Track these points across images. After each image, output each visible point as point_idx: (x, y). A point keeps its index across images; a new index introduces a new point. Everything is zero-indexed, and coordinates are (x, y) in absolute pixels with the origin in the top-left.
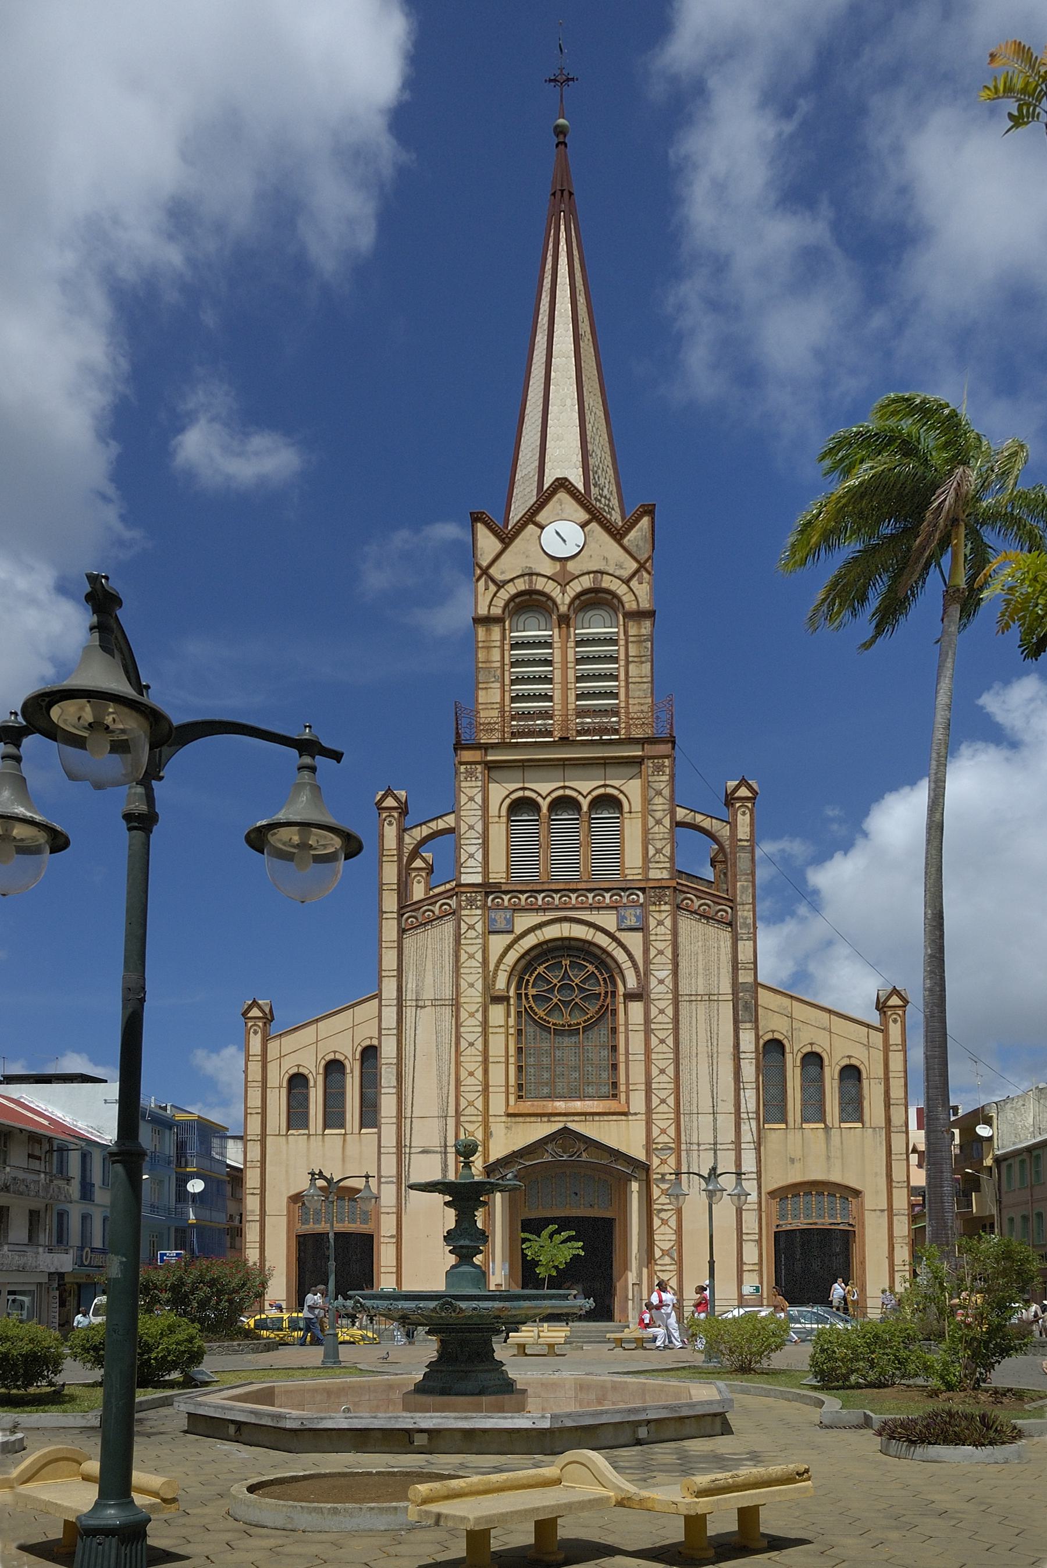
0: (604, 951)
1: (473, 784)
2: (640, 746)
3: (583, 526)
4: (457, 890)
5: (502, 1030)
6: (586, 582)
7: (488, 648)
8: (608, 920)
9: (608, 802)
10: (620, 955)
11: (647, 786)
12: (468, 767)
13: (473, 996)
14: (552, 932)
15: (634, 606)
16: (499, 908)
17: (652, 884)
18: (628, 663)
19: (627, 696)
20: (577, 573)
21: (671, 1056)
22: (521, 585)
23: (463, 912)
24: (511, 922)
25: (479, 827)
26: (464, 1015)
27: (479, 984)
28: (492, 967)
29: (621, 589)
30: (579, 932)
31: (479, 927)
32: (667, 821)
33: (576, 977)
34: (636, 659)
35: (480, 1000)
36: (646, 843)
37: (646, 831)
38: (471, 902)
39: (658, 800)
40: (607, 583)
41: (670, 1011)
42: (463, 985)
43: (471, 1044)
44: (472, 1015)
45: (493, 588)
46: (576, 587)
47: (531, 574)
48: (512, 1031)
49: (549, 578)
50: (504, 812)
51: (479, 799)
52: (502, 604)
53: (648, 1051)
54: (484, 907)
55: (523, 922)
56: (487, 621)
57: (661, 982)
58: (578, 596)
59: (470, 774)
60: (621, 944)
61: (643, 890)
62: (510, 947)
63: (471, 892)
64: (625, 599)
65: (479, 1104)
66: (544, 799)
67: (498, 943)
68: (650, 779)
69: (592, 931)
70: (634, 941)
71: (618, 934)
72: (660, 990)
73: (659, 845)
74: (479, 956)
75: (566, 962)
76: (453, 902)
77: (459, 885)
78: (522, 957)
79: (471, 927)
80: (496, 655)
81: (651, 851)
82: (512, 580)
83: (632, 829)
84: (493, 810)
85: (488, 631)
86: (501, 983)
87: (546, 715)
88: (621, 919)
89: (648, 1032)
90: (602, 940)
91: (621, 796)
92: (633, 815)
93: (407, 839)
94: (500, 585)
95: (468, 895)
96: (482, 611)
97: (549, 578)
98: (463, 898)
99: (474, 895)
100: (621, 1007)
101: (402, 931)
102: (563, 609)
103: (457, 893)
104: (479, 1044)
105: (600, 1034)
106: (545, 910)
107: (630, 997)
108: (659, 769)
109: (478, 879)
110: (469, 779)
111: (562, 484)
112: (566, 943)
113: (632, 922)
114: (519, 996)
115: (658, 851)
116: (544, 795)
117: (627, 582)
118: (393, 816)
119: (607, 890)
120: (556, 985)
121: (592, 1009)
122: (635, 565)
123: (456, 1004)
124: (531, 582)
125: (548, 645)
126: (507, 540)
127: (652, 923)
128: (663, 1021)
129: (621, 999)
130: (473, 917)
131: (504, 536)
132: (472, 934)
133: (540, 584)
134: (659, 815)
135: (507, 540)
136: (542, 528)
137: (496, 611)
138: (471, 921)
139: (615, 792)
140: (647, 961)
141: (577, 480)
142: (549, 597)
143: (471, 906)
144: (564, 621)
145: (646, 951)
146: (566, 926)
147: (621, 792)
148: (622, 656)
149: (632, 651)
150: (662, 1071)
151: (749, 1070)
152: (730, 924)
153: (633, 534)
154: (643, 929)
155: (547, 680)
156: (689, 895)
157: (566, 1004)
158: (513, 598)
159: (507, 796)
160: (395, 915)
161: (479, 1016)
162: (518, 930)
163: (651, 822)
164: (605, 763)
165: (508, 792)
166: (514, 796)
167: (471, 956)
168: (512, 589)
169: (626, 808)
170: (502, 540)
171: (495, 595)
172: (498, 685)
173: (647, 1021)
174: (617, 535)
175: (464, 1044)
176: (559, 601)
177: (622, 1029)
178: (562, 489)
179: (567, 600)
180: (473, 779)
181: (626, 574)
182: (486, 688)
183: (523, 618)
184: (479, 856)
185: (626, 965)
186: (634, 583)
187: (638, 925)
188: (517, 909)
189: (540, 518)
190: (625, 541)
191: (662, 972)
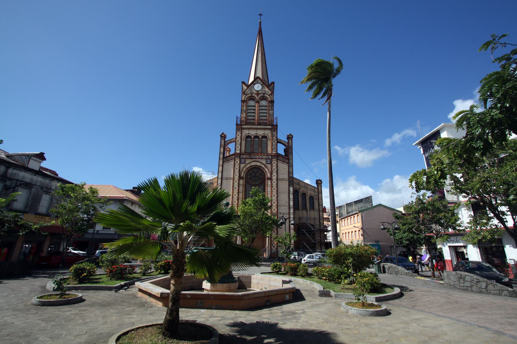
0: (263, 168)
3: (261, 85)
5: (242, 185)
6: (262, 95)
7: (244, 106)
9: (264, 137)
10: (266, 170)
11: (272, 134)
13: (237, 177)
14: (253, 164)
15: (270, 100)
16: (243, 158)
17: (273, 154)
18: (269, 110)
19: (269, 116)
21: (276, 192)
23: (236, 159)
24: (245, 161)
25: (240, 141)
26: (235, 181)
27: (238, 175)
28: (241, 171)
30: (258, 164)
31: (239, 162)
32: (276, 141)
33: (257, 174)
35: (238, 178)
36: (272, 146)
37: (272, 143)
38: (237, 156)
39: (274, 137)
40: (266, 95)
41: (276, 182)
42: (235, 175)
43: (236, 188)
44: (236, 182)
45: (245, 95)
46: (260, 96)
47: (252, 93)
48: (244, 185)
51: (240, 135)
52: (246, 98)
53: (272, 191)
54: (240, 158)
55: (248, 161)
57: (274, 176)
58: (260, 97)
60: (266, 167)
61: (271, 156)
62: (244, 167)
64: (269, 98)
65: (237, 202)
67: (242, 165)
69: (261, 164)
70: (269, 166)
71: (266, 165)
72: (274, 178)
73: (274, 146)
74: (238, 169)
76: (234, 157)
78: (247, 169)
79: (237, 162)
80: (245, 108)
81: (273, 148)
82: (248, 94)
83: (269, 143)
84: (243, 138)
85: (244, 103)
86: (242, 175)
87: (254, 120)
88: (267, 162)
89: (272, 187)
90: (263, 166)
91: (267, 136)
93: (226, 143)
94: (246, 95)
96: (243, 99)
100: (266, 181)
101: (223, 162)
102: (257, 100)
104: (237, 188)
105: (262, 187)
106: (252, 159)
107: (268, 179)
108: (274, 131)
109: (239, 152)
111: (258, 78)
114: (246, 177)
115: (274, 148)
117: (269, 95)
119: (264, 155)
121: (261, 181)
122: (271, 92)
123: (234, 179)
124: (252, 94)
125: (254, 106)
127: (273, 163)
128: (274, 184)
130: (238, 160)
132: (237, 164)
133: (254, 95)
134: (274, 140)
136: (254, 85)
137: (245, 99)
138: (237, 161)
139: (266, 135)
141: (261, 77)
142: (255, 98)
144: (258, 102)
145: (271, 169)
146: (256, 162)
148: (268, 109)
149: (270, 108)
150: (274, 196)
151: (291, 197)
152: (288, 164)
153: (271, 87)
154: (271, 164)
155: (254, 113)
157: (255, 180)
158: (249, 97)
161: (238, 182)
163: (273, 141)
164: (264, 129)
166: (247, 135)
167: (237, 169)
168: (248, 96)
169: (268, 139)
171: (245, 97)
172: (245, 113)
173: (272, 184)
176: (257, 98)
177: (266, 186)
181: (269, 94)
183: (250, 101)
184: (239, 147)
186: (270, 96)
188: (247, 158)
189: (254, 83)
190: (269, 88)
191: (275, 174)
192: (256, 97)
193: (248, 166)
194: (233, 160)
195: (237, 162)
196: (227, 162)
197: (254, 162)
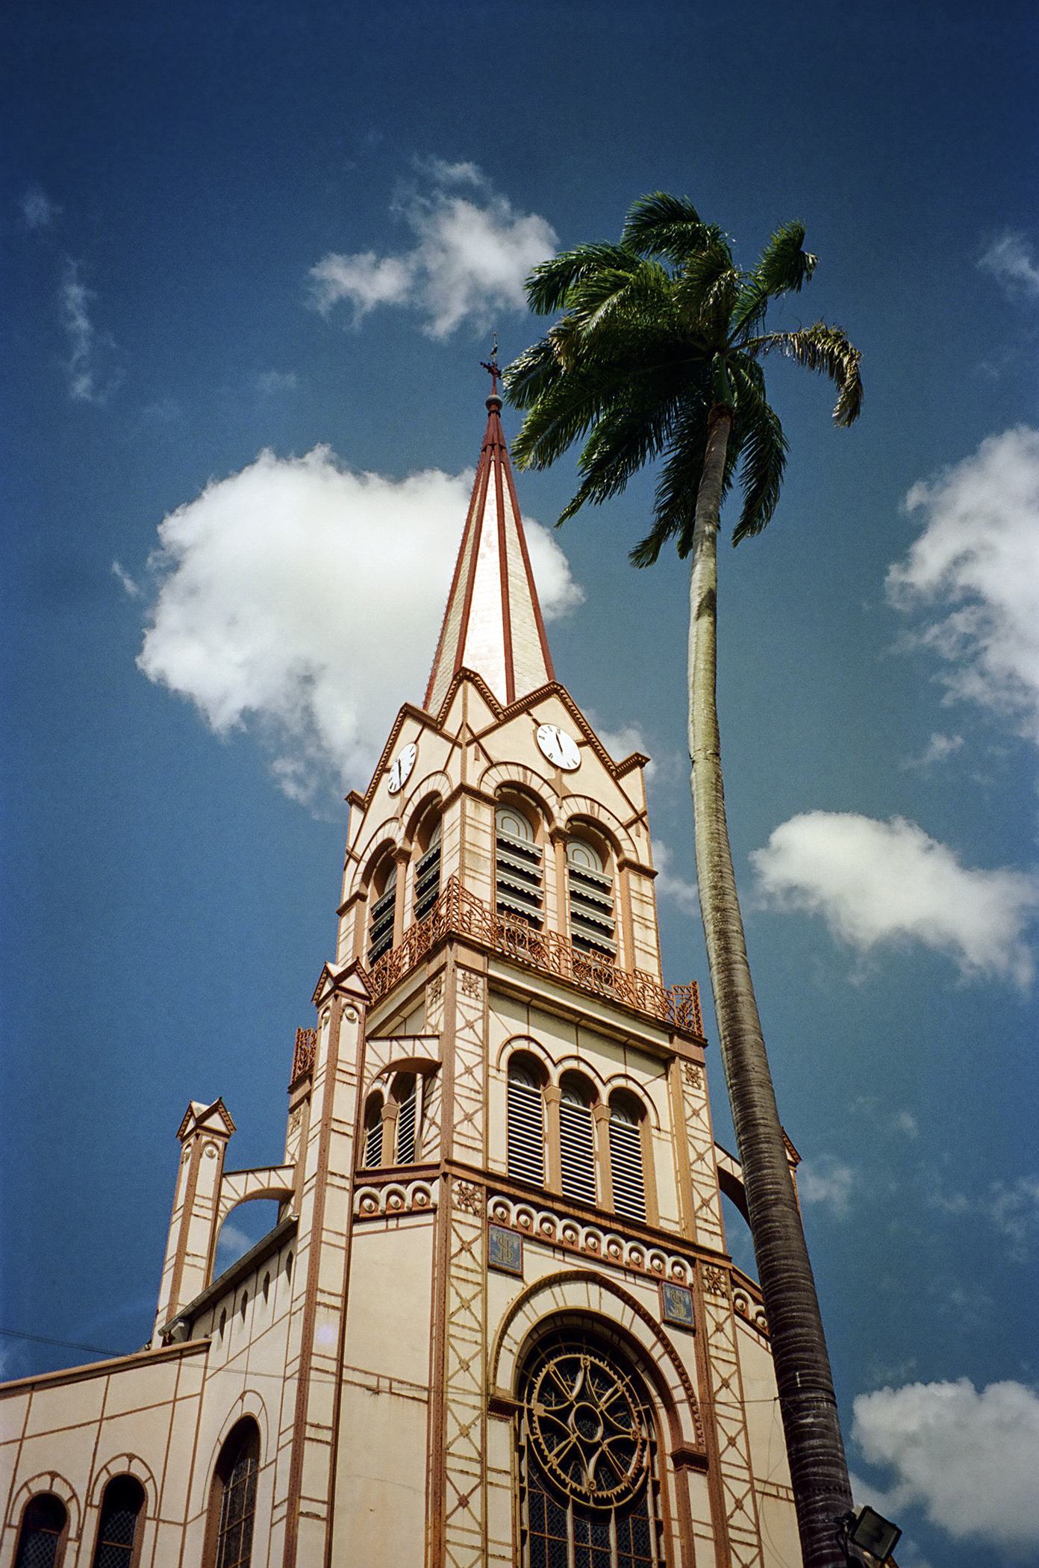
1: (473, 1003)
2: (667, 1037)
4: (447, 1168)
8: (649, 1297)
12: (467, 974)
14: (578, 1296)
20: (574, 793)
22: (515, 774)
29: (620, 834)
30: (612, 1308)
34: (640, 920)
38: (467, 1199)
49: (545, 781)
50: (504, 1066)
55: (539, 1264)
56: (477, 795)
59: (470, 987)
61: (692, 1261)
63: (467, 1181)
66: (555, 1065)
68: (685, 1088)
69: (629, 1312)
71: (668, 1331)
75: (586, 1360)
76: (435, 1189)
77: (450, 1162)
88: (666, 1304)
90: (645, 1336)
91: (645, 1100)
92: (663, 1135)
94: (493, 765)
95: (464, 1184)
97: (545, 781)
98: (456, 1187)
99: (471, 1186)
100: (671, 1478)
103: (445, 1175)
106: (565, 1251)
107: (689, 1460)
110: (467, 992)
112: (588, 1323)
113: (679, 1314)
116: (555, 1060)
117: (626, 827)
118: (356, 1009)
120: (597, 1407)
126: (501, 717)
129: (670, 1464)
130: (467, 1227)
131: (499, 710)
135: (501, 717)
137: (488, 790)
138: (468, 1235)
140: (710, 1399)
143: (467, 1205)
146: (594, 1289)
147: (646, 1093)
156: (743, 1292)
159: (509, 1042)
160: (347, 1184)
162: (532, 1278)
165: (508, 1037)
170: (496, 715)
171: (486, 771)
174: (617, 773)
175: (451, 1500)
176: (555, 810)
178: (555, 695)
179: (565, 818)
180: (473, 995)
182: (474, 878)
185: (679, 1394)
186: (632, 831)
187: (688, 1321)
192: (552, 802)
193: (544, 1305)
194: (429, 1218)
195: (465, 1247)
196: (381, 1225)
197: (581, 1287)
